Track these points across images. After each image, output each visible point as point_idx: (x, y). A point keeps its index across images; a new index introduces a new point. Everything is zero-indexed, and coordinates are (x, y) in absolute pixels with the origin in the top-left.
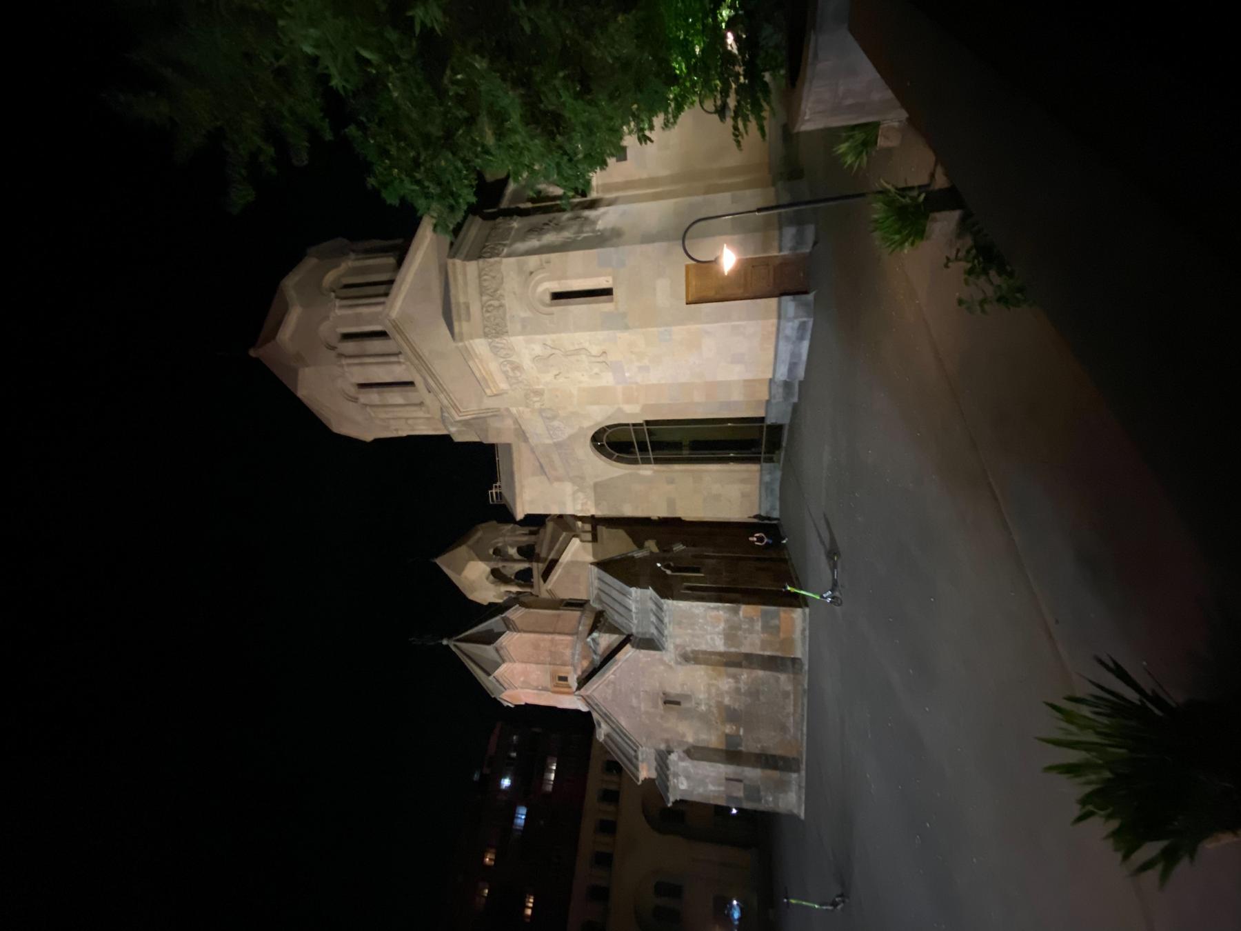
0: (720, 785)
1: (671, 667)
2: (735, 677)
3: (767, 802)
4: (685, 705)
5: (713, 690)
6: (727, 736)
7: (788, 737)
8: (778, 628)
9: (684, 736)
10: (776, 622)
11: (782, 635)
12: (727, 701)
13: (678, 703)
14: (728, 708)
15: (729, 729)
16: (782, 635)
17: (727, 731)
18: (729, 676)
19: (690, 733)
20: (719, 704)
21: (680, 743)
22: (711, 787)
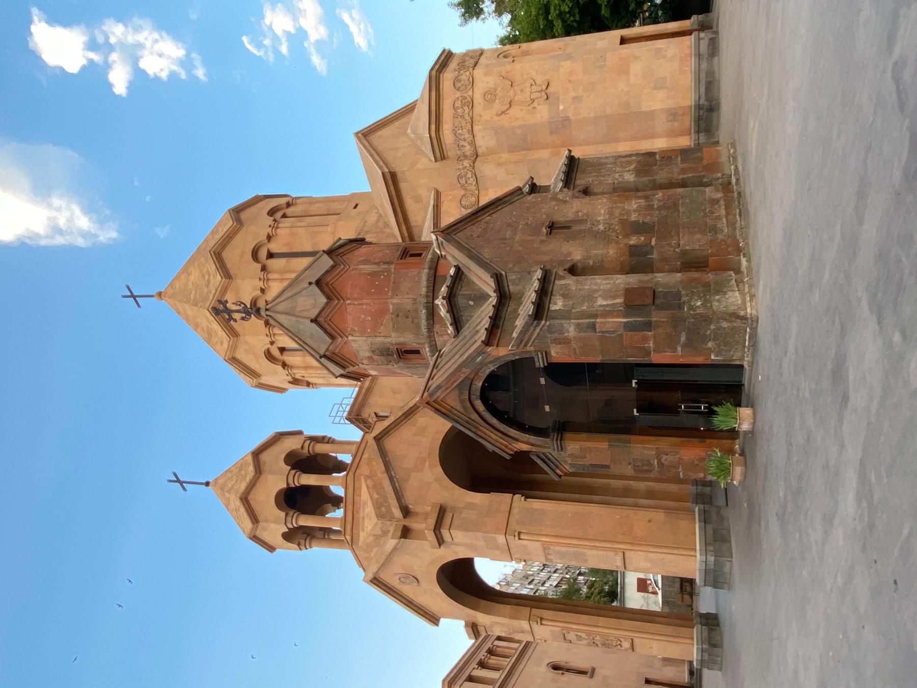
0: (614, 297)
1: (565, 202)
2: (646, 198)
3: (691, 308)
4: (576, 228)
5: (617, 212)
6: (631, 246)
7: (720, 237)
8: (701, 159)
9: (569, 254)
10: (699, 154)
11: (705, 162)
12: (633, 217)
13: (569, 228)
14: (636, 223)
15: (633, 241)
16: (705, 162)
17: (632, 242)
18: (640, 198)
19: (577, 254)
20: (623, 222)
21: (561, 263)
22: (601, 302)
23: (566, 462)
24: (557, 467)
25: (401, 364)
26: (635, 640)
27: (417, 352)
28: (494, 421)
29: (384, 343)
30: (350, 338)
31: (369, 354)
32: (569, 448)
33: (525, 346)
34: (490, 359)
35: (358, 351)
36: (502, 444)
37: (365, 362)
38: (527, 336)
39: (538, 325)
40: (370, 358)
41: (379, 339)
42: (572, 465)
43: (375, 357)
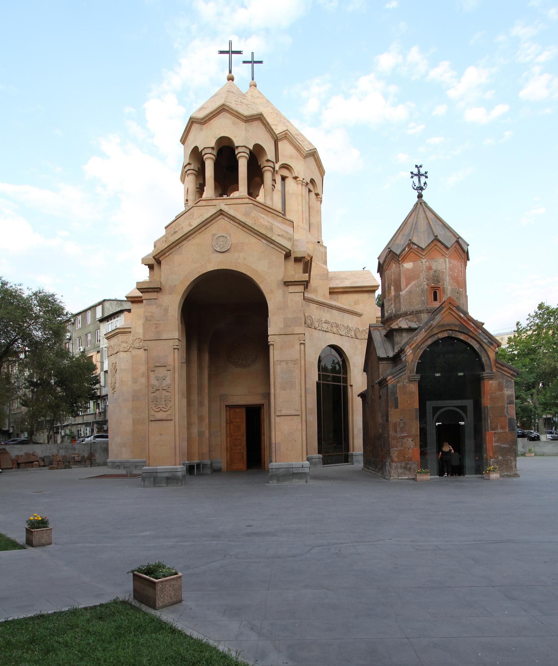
23: (398, 382)
24: (393, 377)
25: (426, 287)
26: (172, 422)
27: (435, 299)
28: (429, 342)
29: (443, 280)
30: (447, 260)
31: (434, 267)
32: (412, 385)
33: (497, 367)
34: (485, 347)
35: (436, 261)
36: (413, 344)
37: (427, 263)
38: (506, 369)
39: (512, 375)
40: (430, 268)
41: (448, 278)
42: (395, 386)
43: (432, 272)
